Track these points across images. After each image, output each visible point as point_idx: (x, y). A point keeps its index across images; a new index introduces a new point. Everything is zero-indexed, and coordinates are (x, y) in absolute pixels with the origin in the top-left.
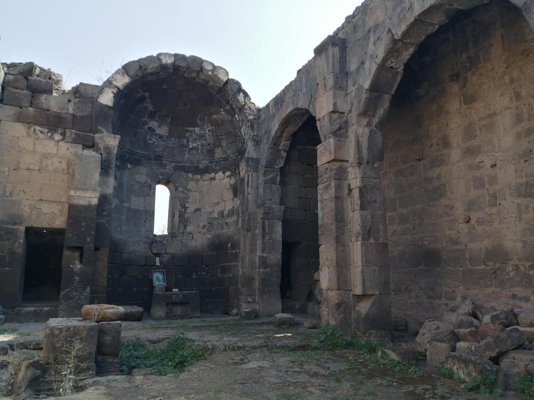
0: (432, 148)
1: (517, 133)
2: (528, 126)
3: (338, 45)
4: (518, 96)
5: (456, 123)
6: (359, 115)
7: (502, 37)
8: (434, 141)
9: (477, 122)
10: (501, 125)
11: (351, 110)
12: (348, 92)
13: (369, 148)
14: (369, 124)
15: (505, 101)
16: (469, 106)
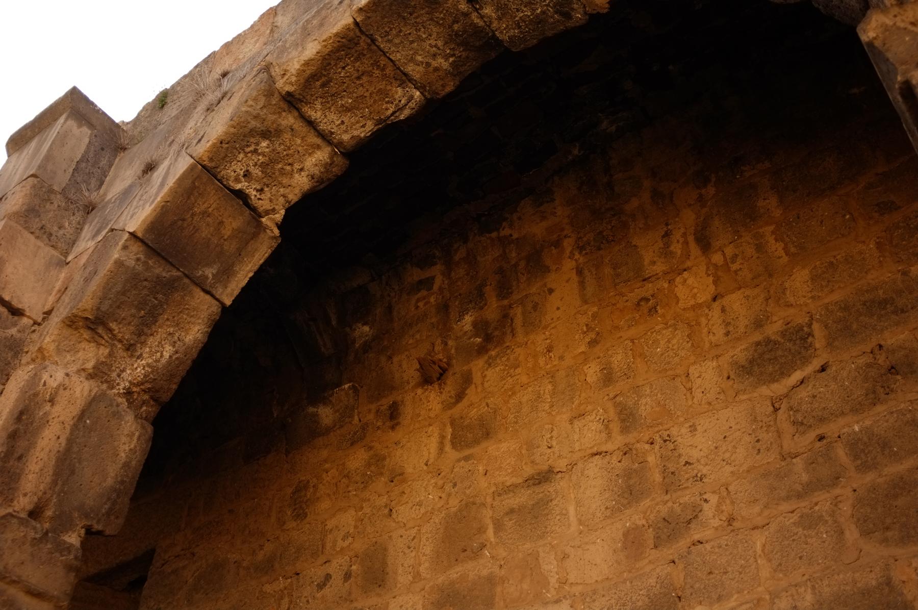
0: (326, 591)
1: (626, 535)
2: (664, 510)
3: (91, 126)
4: (627, 419)
5: (420, 504)
6: (71, 322)
7: (580, 272)
8: (336, 567)
9: (489, 500)
10: (572, 510)
11: (48, 313)
12: (70, 258)
13: (66, 464)
14: (99, 373)
15: (589, 433)
16: (467, 452)
